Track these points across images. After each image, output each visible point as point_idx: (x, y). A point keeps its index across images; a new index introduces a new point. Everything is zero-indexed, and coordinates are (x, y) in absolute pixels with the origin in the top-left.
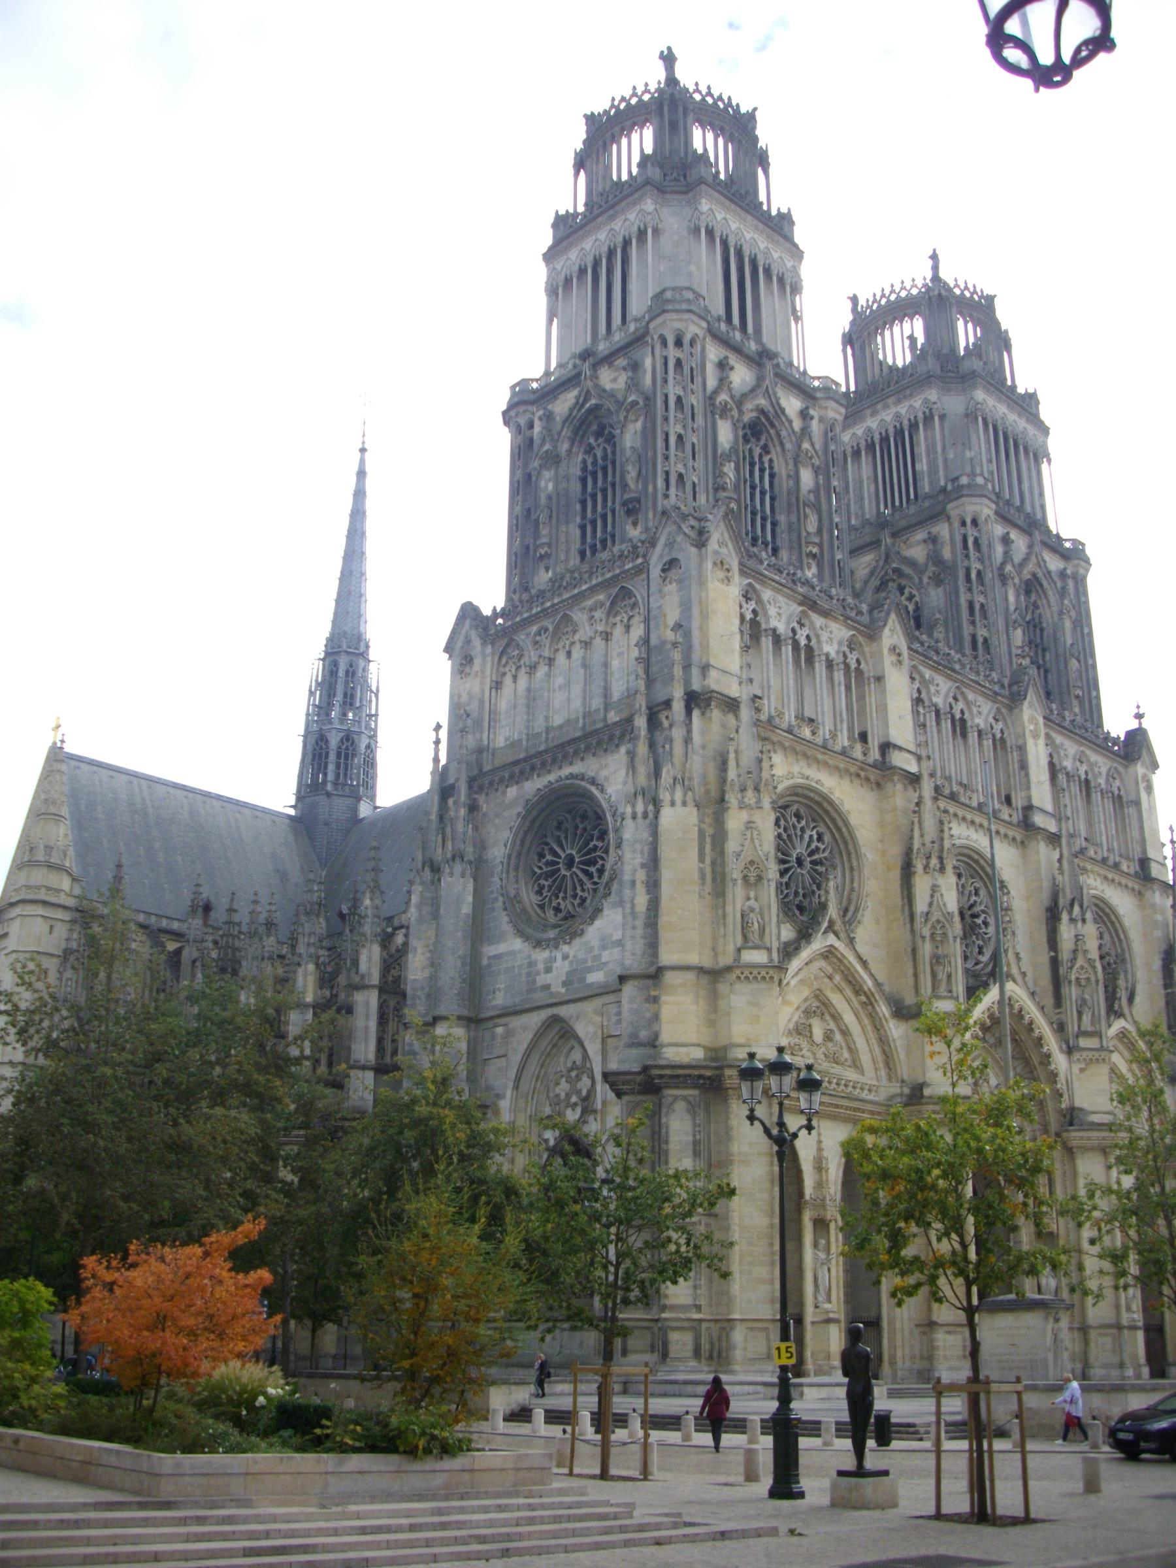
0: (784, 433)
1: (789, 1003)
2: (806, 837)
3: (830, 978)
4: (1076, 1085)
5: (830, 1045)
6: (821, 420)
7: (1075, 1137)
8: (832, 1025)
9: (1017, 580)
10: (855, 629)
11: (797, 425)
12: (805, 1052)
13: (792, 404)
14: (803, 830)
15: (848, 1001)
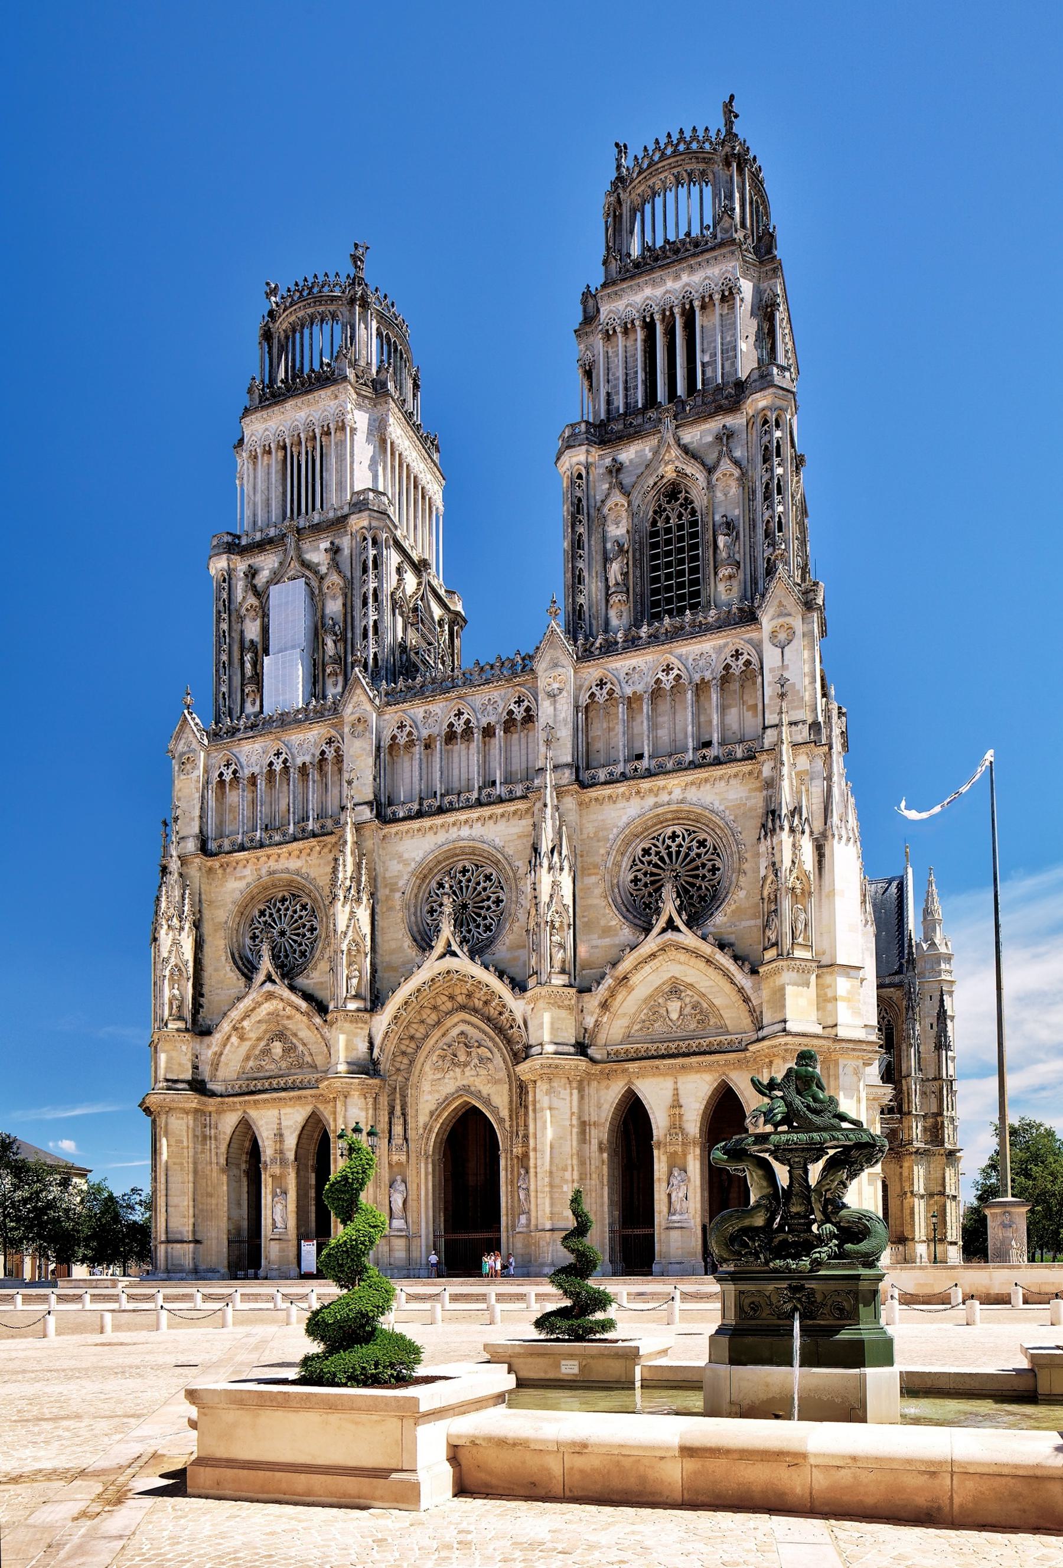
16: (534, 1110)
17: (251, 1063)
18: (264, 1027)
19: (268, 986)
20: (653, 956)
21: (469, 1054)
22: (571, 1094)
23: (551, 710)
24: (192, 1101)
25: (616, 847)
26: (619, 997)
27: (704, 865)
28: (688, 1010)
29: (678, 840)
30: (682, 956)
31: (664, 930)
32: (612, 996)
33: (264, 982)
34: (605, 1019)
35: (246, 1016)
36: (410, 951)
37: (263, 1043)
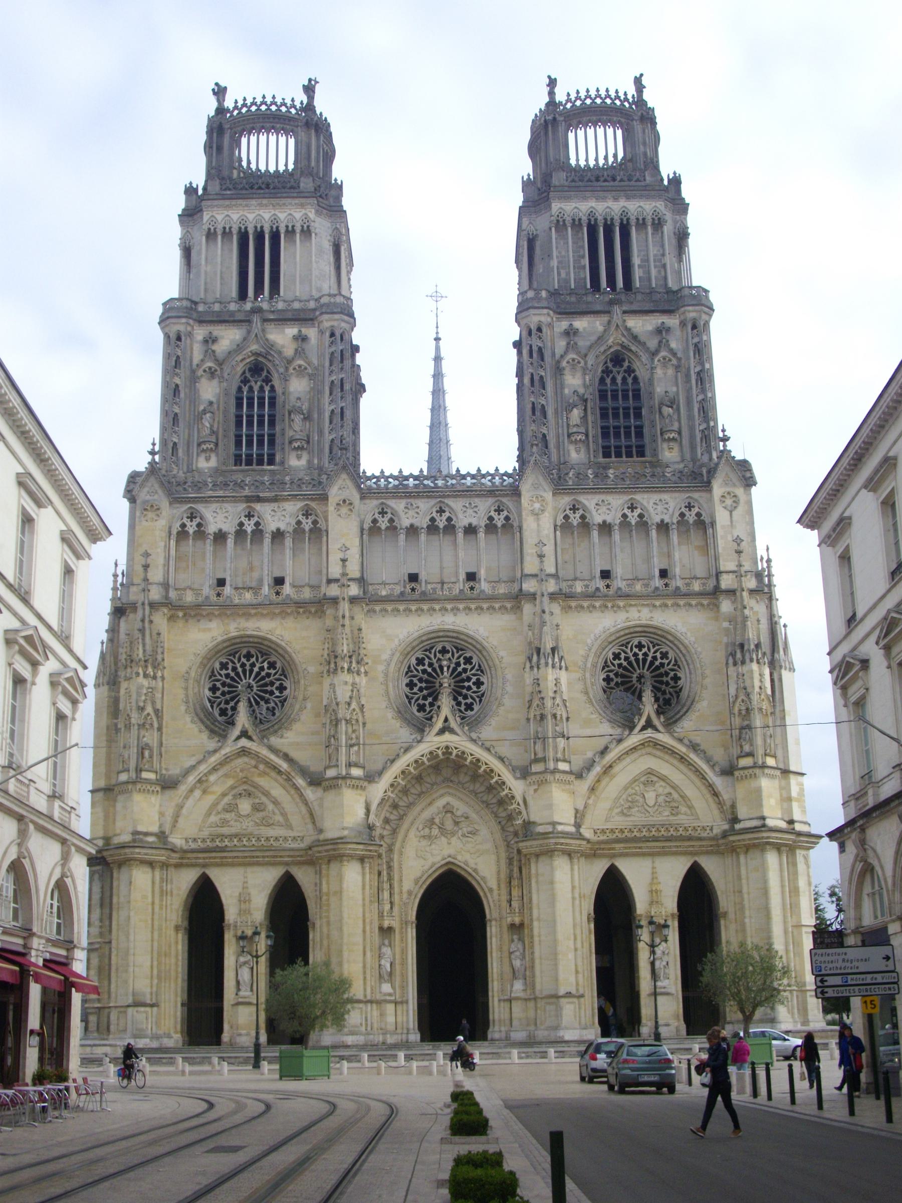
0: (277, 362)
1: (213, 793)
2: (256, 669)
3: (256, 767)
4: (530, 802)
5: (261, 814)
6: (321, 332)
7: (528, 846)
8: (264, 799)
9: (582, 362)
10: (304, 499)
11: (289, 352)
12: (232, 823)
13: (283, 337)
14: (253, 665)
15: (276, 780)
16: (537, 882)
17: (213, 819)
18: (230, 782)
19: (244, 742)
20: (634, 749)
21: (457, 823)
22: (572, 869)
23: (534, 525)
24: (160, 856)
25: (593, 650)
26: (604, 783)
27: (667, 674)
28: (661, 799)
29: (645, 650)
30: (658, 753)
31: (644, 728)
32: (598, 781)
33: (238, 738)
34: (591, 802)
35: (214, 769)
36: (394, 721)
37: (230, 797)
